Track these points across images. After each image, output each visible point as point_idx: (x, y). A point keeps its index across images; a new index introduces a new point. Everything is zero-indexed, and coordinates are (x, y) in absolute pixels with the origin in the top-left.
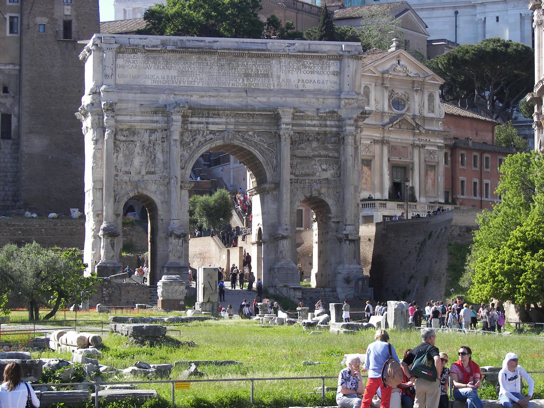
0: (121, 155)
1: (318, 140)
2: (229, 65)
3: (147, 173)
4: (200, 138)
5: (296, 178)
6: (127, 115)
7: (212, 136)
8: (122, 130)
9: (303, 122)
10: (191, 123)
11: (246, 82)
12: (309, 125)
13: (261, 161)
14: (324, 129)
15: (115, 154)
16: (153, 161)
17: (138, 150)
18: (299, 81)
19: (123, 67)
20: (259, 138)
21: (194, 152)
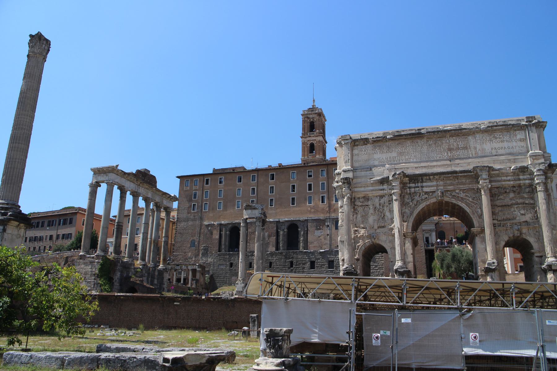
0: (359, 216)
1: (514, 192)
2: (435, 144)
3: (379, 227)
4: (417, 198)
5: (499, 222)
6: (361, 187)
7: (426, 196)
8: (359, 198)
9: (500, 179)
10: (410, 188)
11: (449, 155)
12: (505, 181)
13: (468, 211)
14: (518, 182)
15: (355, 216)
16: (383, 218)
17: (371, 211)
18: (492, 149)
19: (358, 155)
20: (464, 194)
21: (414, 209)
